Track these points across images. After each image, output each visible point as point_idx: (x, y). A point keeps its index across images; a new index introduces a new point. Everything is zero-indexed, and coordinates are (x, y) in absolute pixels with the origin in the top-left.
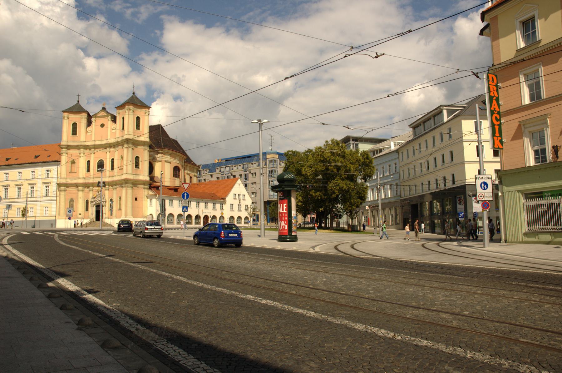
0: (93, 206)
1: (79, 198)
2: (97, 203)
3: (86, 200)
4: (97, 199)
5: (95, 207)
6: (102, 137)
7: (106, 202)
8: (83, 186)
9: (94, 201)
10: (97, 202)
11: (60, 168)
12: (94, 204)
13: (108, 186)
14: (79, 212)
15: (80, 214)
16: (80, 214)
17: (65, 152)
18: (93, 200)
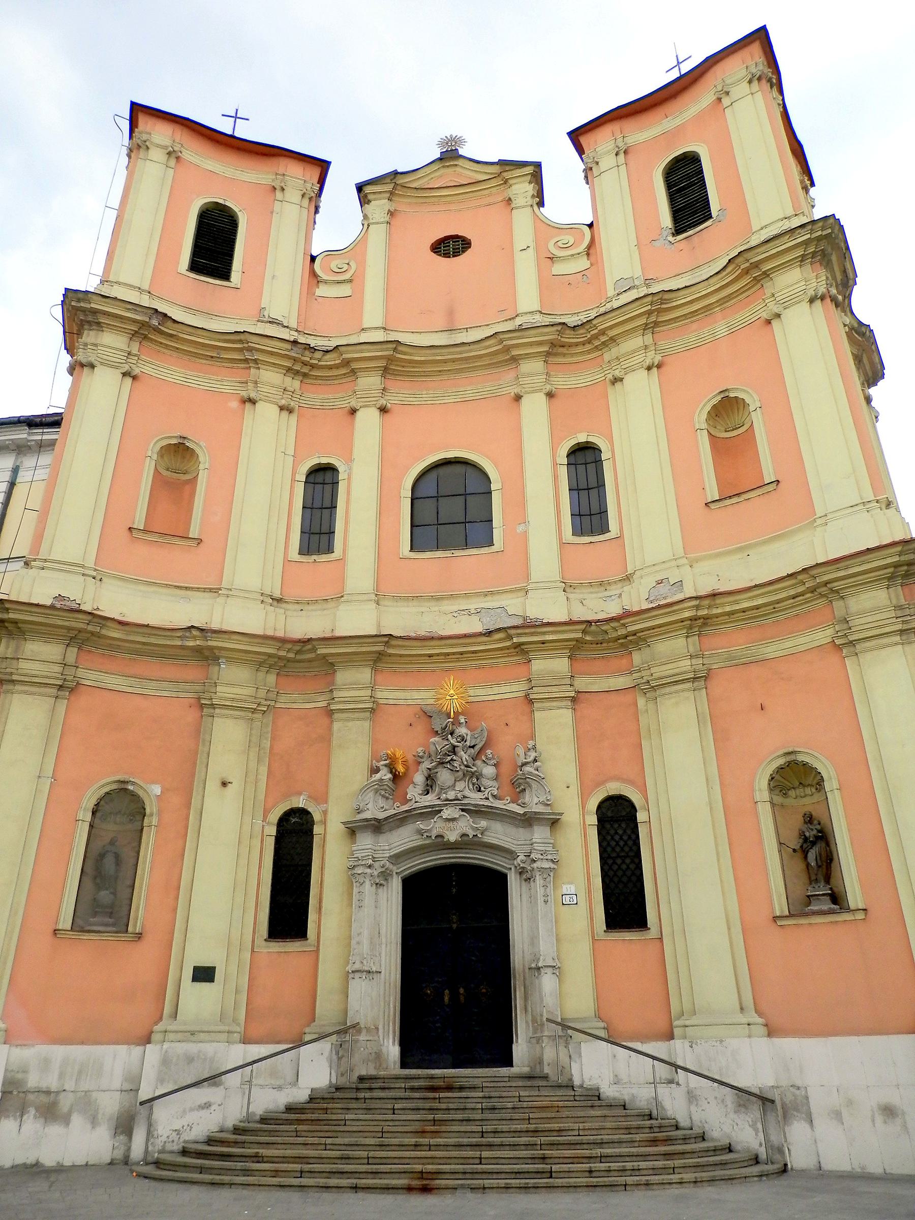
0: (386, 875)
1: (212, 785)
2: (441, 844)
3: (275, 816)
4: (430, 799)
5: (396, 886)
6: (451, 313)
7: (554, 823)
8: (264, 663)
9: (401, 820)
10: (435, 826)
11: (38, 490)
12: (396, 858)
13: (560, 665)
14: (198, 956)
15: (204, 974)
16: (204, 974)
17: (119, 357)
18: (376, 809)
